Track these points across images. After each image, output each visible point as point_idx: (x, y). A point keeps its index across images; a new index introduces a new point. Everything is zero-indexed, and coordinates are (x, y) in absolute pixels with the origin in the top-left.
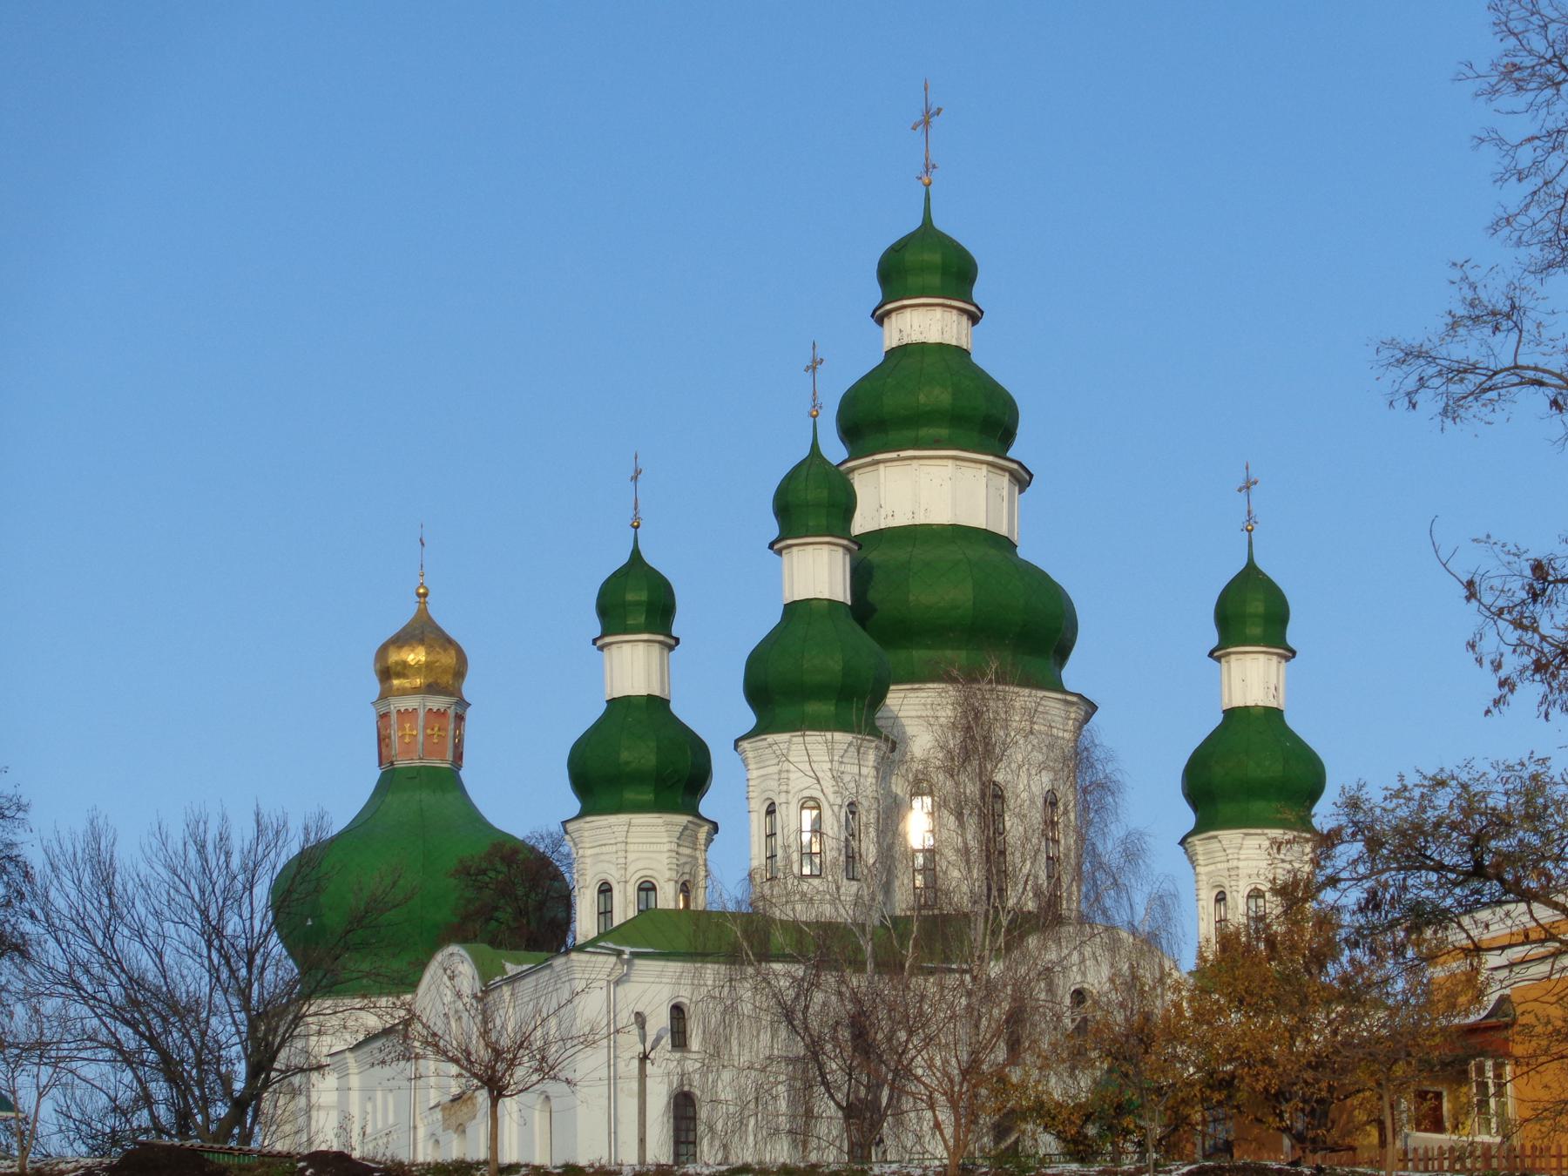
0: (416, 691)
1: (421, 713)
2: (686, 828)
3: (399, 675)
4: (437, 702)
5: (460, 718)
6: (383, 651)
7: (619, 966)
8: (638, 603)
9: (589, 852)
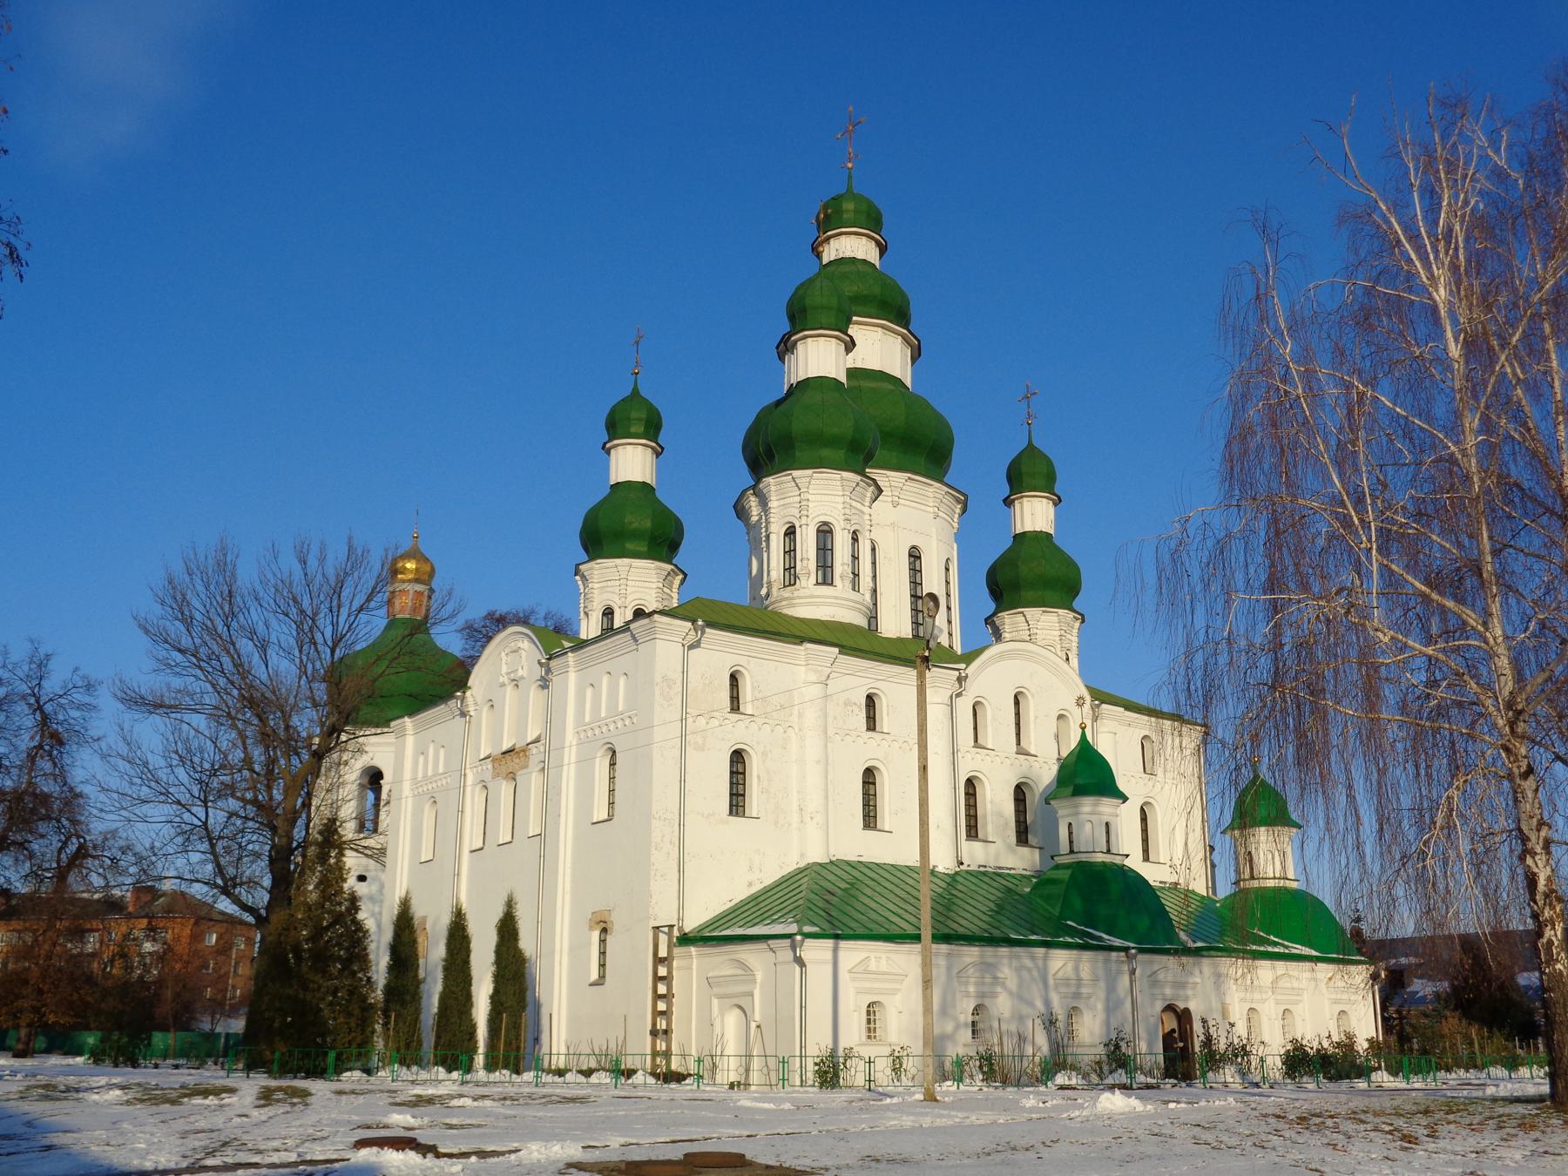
0: (410, 581)
1: (411, 592)
2: (669, 574)
3: (402, 573)
4: (420, 587)
5: (430, 597)
6: (395, 561)
7: (693, 632)
8: (640, 420)
9: (596, 586)
